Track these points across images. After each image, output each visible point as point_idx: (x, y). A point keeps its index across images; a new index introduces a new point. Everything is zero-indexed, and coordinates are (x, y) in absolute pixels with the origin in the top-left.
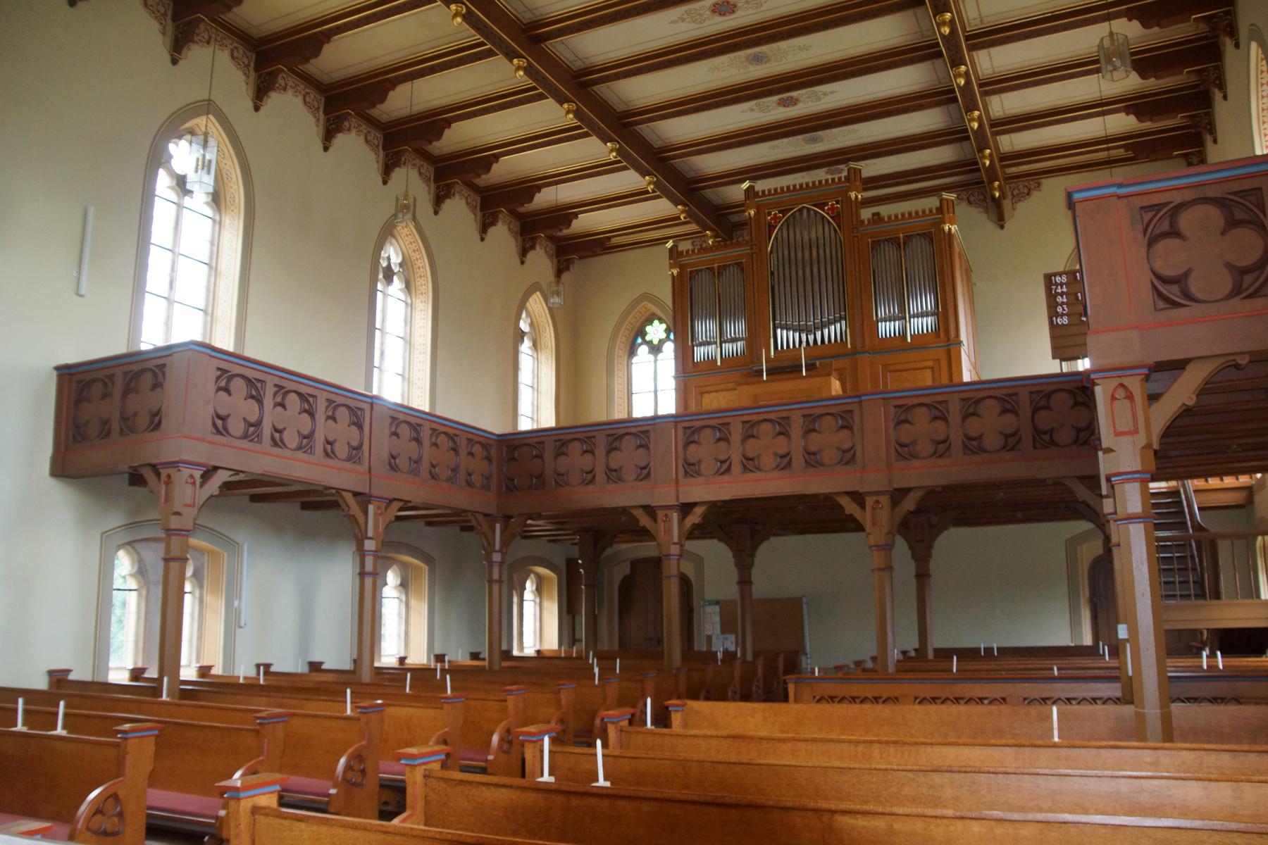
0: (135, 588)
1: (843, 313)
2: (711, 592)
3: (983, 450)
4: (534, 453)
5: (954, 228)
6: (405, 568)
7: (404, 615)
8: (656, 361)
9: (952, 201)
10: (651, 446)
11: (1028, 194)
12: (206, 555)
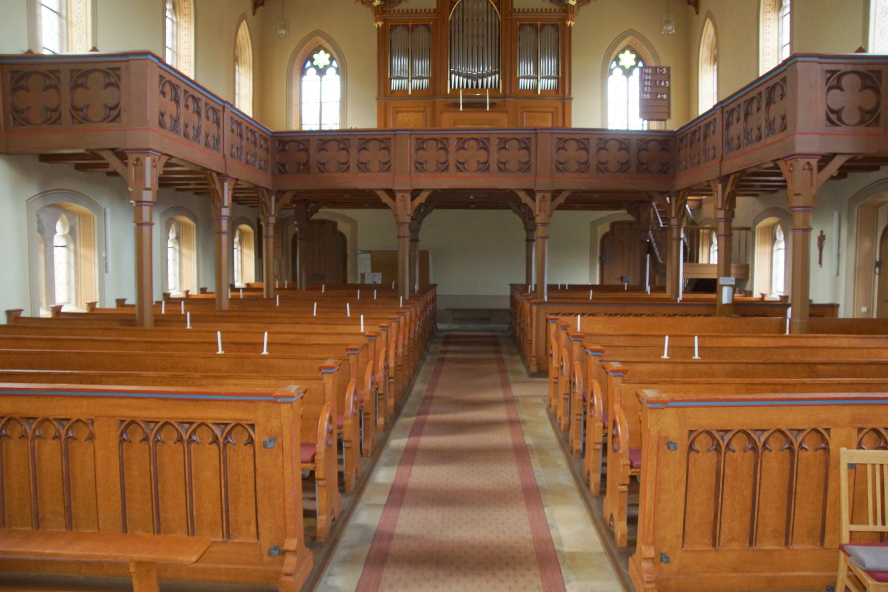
0: (64, 245)
1: (497, 70)
2: (362, 245)
3: (607, 170)
4: (301, 147)
5: (573, 23)
6: (179, 224)
7: (178, 260)
8: (321, 81)
10: (392, 149)
12: (77, 216)
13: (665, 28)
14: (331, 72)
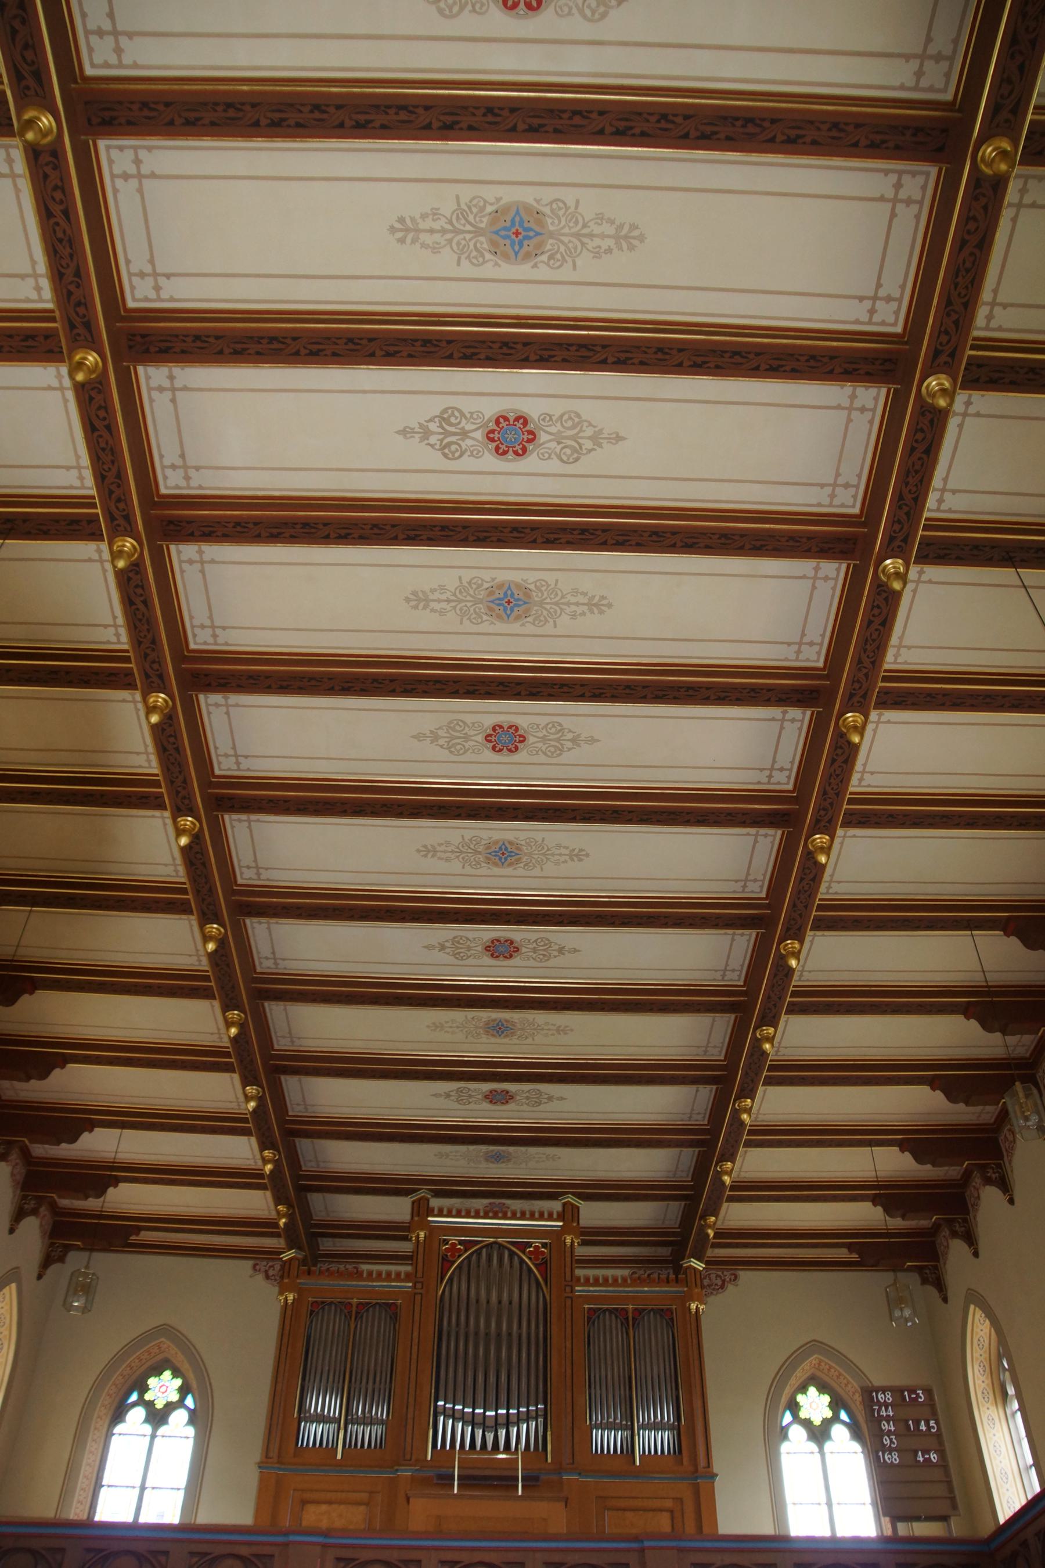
8: (153, 1436)
9: (700, 1272)
11: (722, 1287)
13: (897, 1313)
14: (179, 1418)
